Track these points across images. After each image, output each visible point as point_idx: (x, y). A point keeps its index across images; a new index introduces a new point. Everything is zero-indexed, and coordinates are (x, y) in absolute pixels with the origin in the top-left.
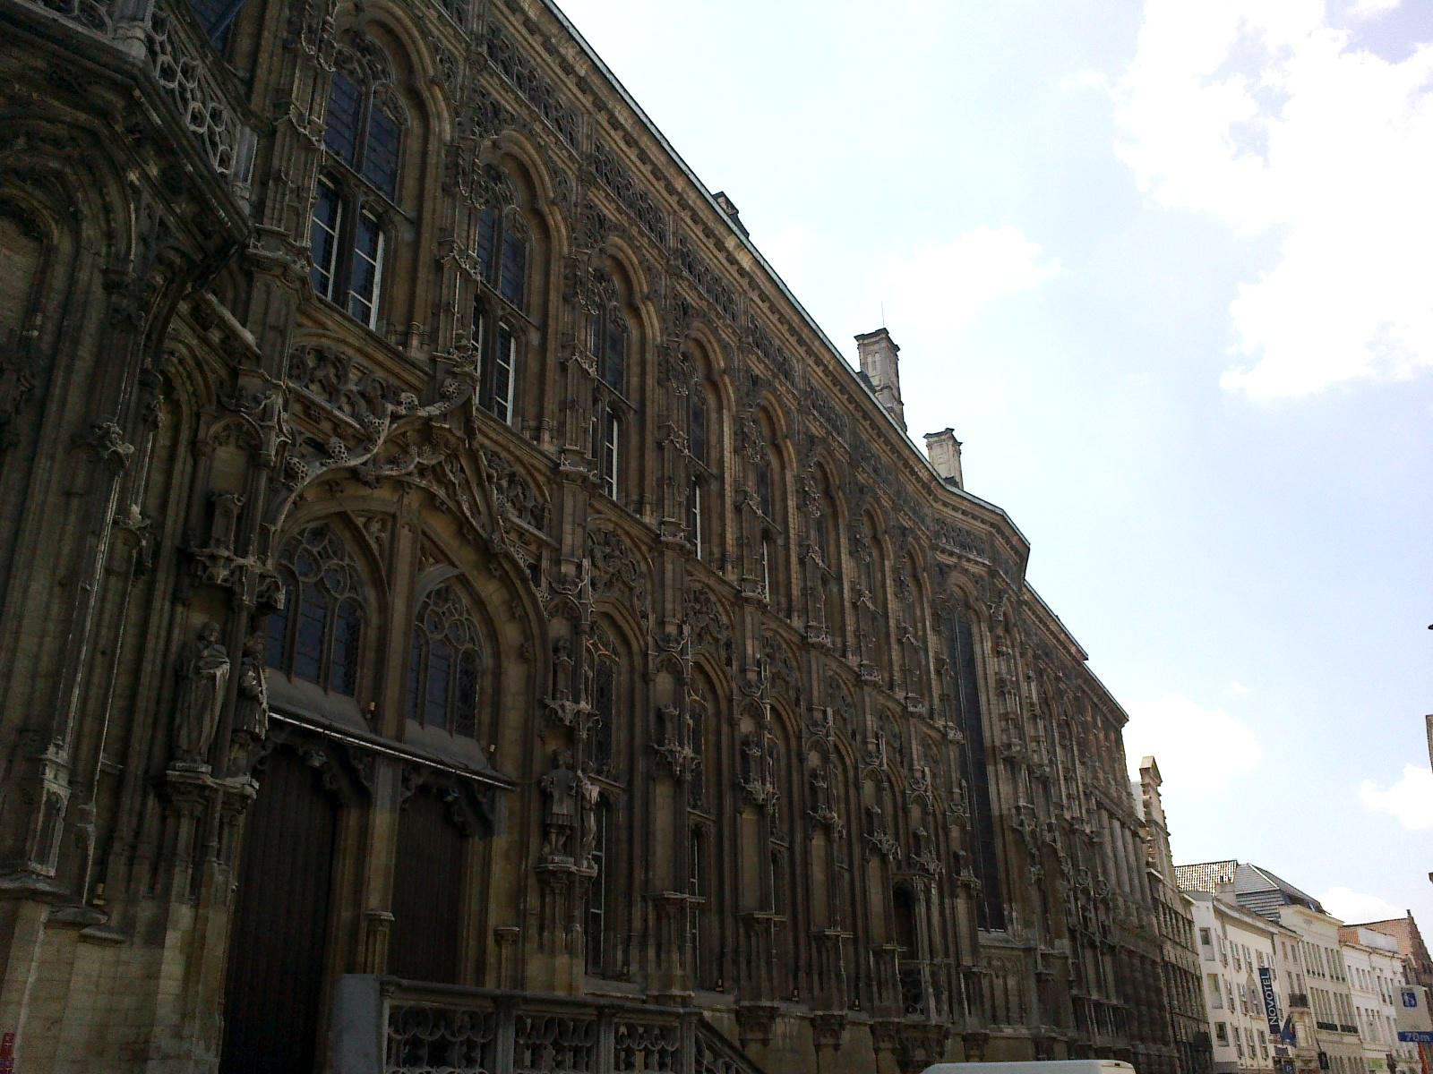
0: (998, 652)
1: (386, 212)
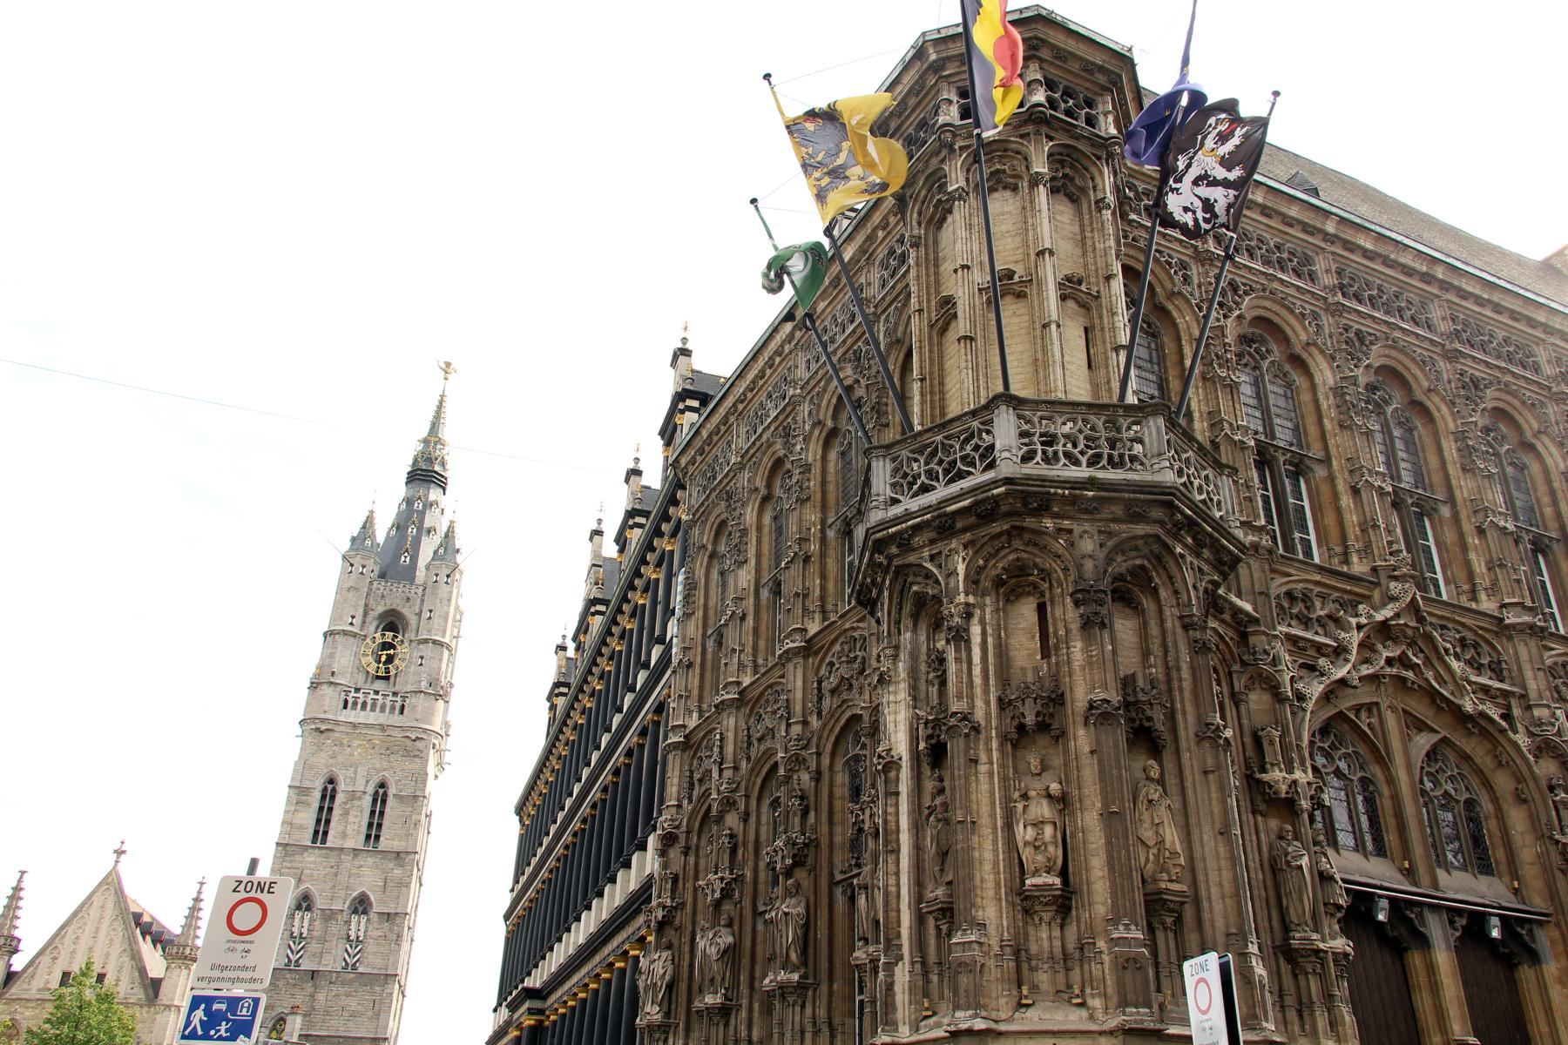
1: (1301, 461)
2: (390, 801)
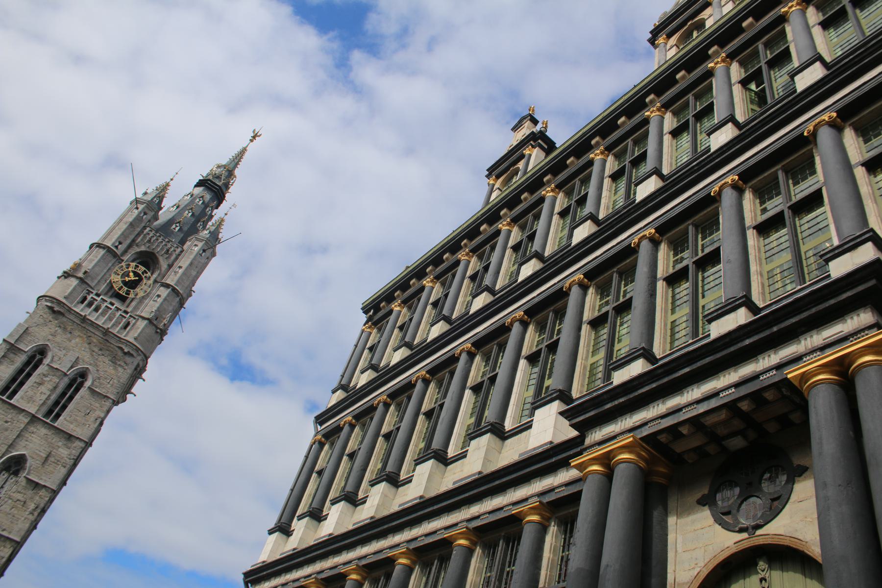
2: (83, 391)
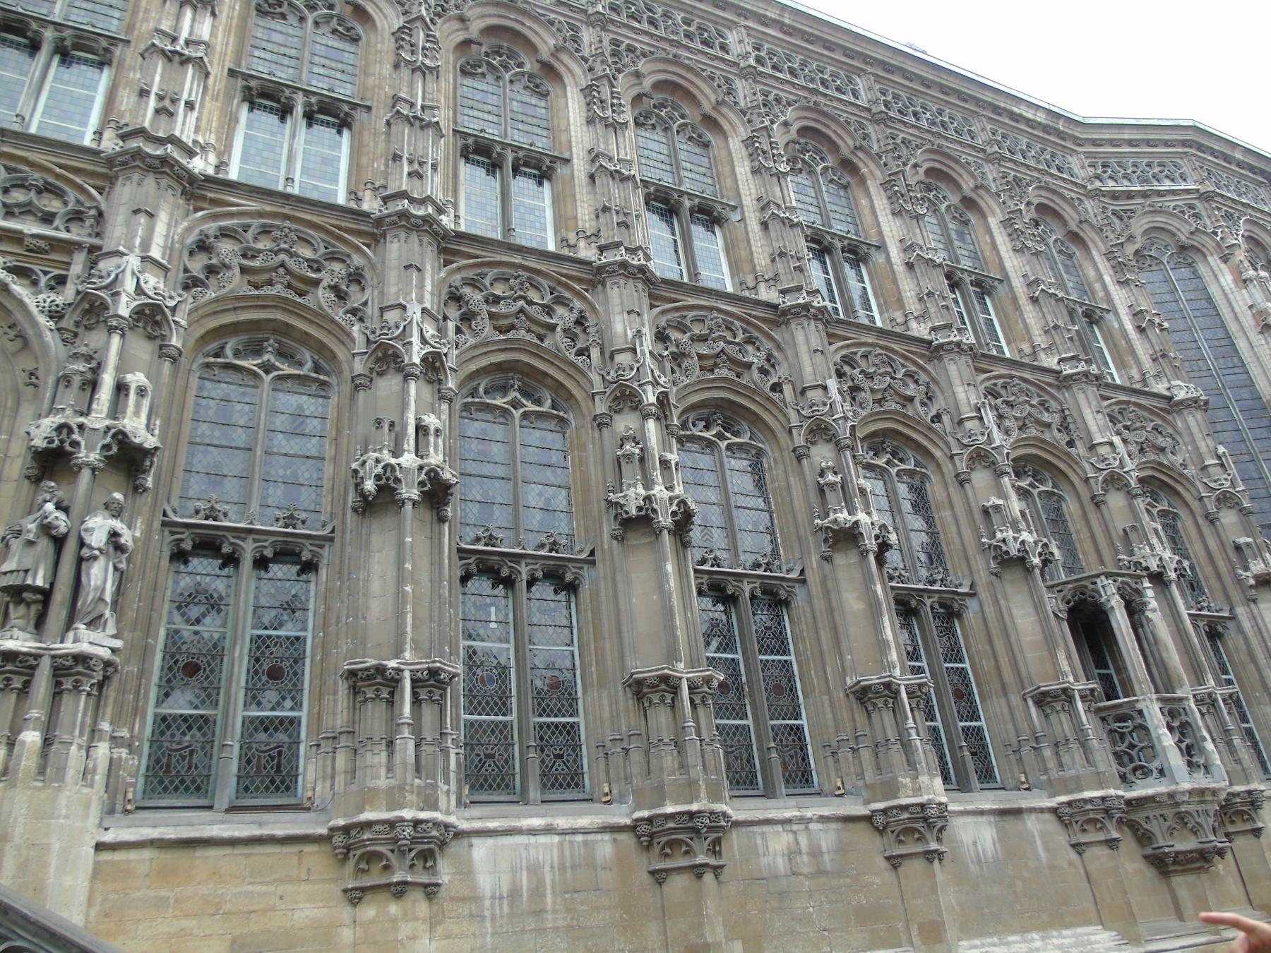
0: (1245, 281)
